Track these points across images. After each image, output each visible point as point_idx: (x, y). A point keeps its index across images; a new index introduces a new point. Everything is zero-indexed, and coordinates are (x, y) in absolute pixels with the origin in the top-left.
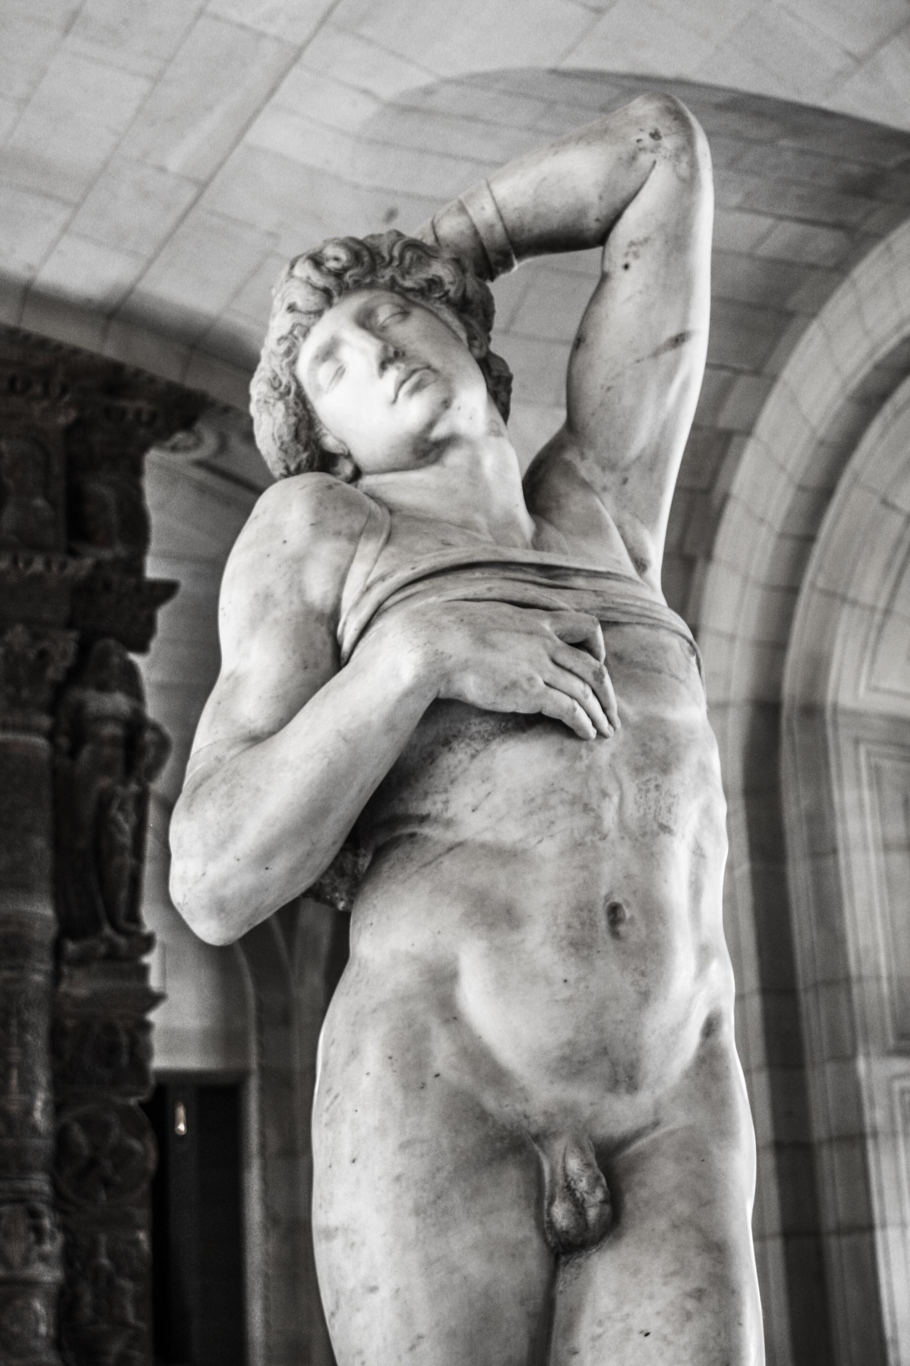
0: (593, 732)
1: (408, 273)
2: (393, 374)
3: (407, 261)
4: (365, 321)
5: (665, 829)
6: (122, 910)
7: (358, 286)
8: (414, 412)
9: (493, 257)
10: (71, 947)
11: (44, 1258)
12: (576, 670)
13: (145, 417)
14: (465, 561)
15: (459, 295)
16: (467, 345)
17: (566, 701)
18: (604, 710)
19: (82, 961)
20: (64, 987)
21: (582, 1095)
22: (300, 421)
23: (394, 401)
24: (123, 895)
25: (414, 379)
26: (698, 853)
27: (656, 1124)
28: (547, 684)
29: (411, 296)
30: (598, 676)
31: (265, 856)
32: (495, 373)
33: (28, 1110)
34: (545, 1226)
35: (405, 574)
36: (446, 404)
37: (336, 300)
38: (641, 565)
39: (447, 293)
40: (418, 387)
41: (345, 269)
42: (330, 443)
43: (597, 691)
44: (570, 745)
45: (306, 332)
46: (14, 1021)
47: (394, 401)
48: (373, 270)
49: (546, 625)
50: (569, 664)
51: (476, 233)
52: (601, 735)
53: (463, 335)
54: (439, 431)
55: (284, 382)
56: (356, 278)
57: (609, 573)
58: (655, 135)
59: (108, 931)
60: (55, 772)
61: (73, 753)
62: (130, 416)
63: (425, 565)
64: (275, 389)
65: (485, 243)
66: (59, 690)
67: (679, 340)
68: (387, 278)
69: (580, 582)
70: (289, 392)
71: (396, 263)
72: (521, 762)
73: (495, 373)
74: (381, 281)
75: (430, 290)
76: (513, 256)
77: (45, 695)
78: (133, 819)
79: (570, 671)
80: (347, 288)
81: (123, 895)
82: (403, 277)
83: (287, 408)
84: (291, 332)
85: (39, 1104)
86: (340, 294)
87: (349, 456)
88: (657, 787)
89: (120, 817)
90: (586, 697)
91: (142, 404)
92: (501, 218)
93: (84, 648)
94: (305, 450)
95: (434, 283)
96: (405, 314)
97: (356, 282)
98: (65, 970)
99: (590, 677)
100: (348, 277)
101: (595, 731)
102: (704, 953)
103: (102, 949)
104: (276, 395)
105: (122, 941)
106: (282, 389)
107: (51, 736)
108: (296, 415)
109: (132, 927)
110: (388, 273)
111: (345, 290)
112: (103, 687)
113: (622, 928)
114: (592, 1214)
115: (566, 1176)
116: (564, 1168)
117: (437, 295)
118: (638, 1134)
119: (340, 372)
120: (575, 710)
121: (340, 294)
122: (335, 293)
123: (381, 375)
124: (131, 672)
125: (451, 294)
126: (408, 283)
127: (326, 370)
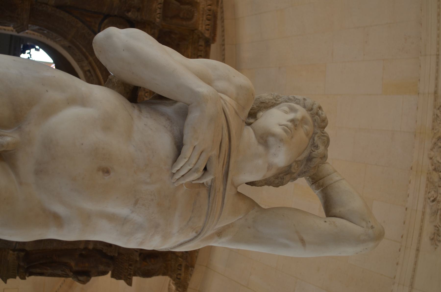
0: (174, 171)
1: (319, 139)
2: (289, 124)
3: (323, 138)
4: (303, 120)
5: (136, 203)
7: (314, 121)
8: (278, 130)
9: (321, 181)
10: (23, 254)
12: (199, 161)
13: (179, 277)
14: (232, 135)
15: (314, 156)
16: (297, 160)
17: (188, 155)
18: (183, 176)
20: (11, 252)
22: (267, 104)
23: (280, 125)
24: (38, 271)
25: (289, 130)
26: (124, 221)
27: (21, 183)
28: (195, 147)
29: (312, 140)
30: (197, 171)
31: (129, 49)
32: (285, 177)
36: (281, 140)
37: (309, 112)
38: (219, 234)
39: (314, 151)
40: (285, 131)
41: (319, 116)
42: (260, 114)
43: (190, 171)
44: (170, 161)
45: (297, 103)
47: (280, 125)
49: (215, 152)
50: (202, 158)
51: (329, 175)
53: (300, 158)
54: (271, 140)
55: (280, 100)
56: (317, 120)
57: (224, 204)
58: (372, 227)
62: (179, 272)
63: (231, 119)
64: (277, 97)
65: (325, 178)
67: (303, 242)
68: (317, 131)
69: (222, 189)
70: (276, 101)
71: (322, 134)
72: (164, 142)
73: (285, 177)
74: (316, 129)
75: (315, 146)
76: (322, 189)
79: (199, 159)
80: (313, 117)
81: (38, 271)
82: (318, 137)
83: (271, 99)
84: (297, 99)
86: (311, 114)
87: (256, 120)
88: (152, 200)
90: (189, 166)
91: (183, 275)
92: (335, 182)
93: (112, 258)
94: (257, 106)
95: (317, 147)
96: (307, 135)
97: (315, 120)
98: (16, 253)
99: (196, 167)
100: (317, 116)
101: (175, 172)
102: (87, 218)
104: (275, 97)
106: (277, 99)
108: (269, 102)
109: (28, 275)
110: (319, 131)
111: (312, 116)
113: (101, 173)
115: (4, 136)
116: (7, 136)
117: (313, 149)
118: (17, 174)
119: (286, 112)
120: (185, 158)
121: (311, 114)
122: (311, 112)
123: (288, 121)
125: (314, 153)
126: (316, 138)
127: (286, 108)
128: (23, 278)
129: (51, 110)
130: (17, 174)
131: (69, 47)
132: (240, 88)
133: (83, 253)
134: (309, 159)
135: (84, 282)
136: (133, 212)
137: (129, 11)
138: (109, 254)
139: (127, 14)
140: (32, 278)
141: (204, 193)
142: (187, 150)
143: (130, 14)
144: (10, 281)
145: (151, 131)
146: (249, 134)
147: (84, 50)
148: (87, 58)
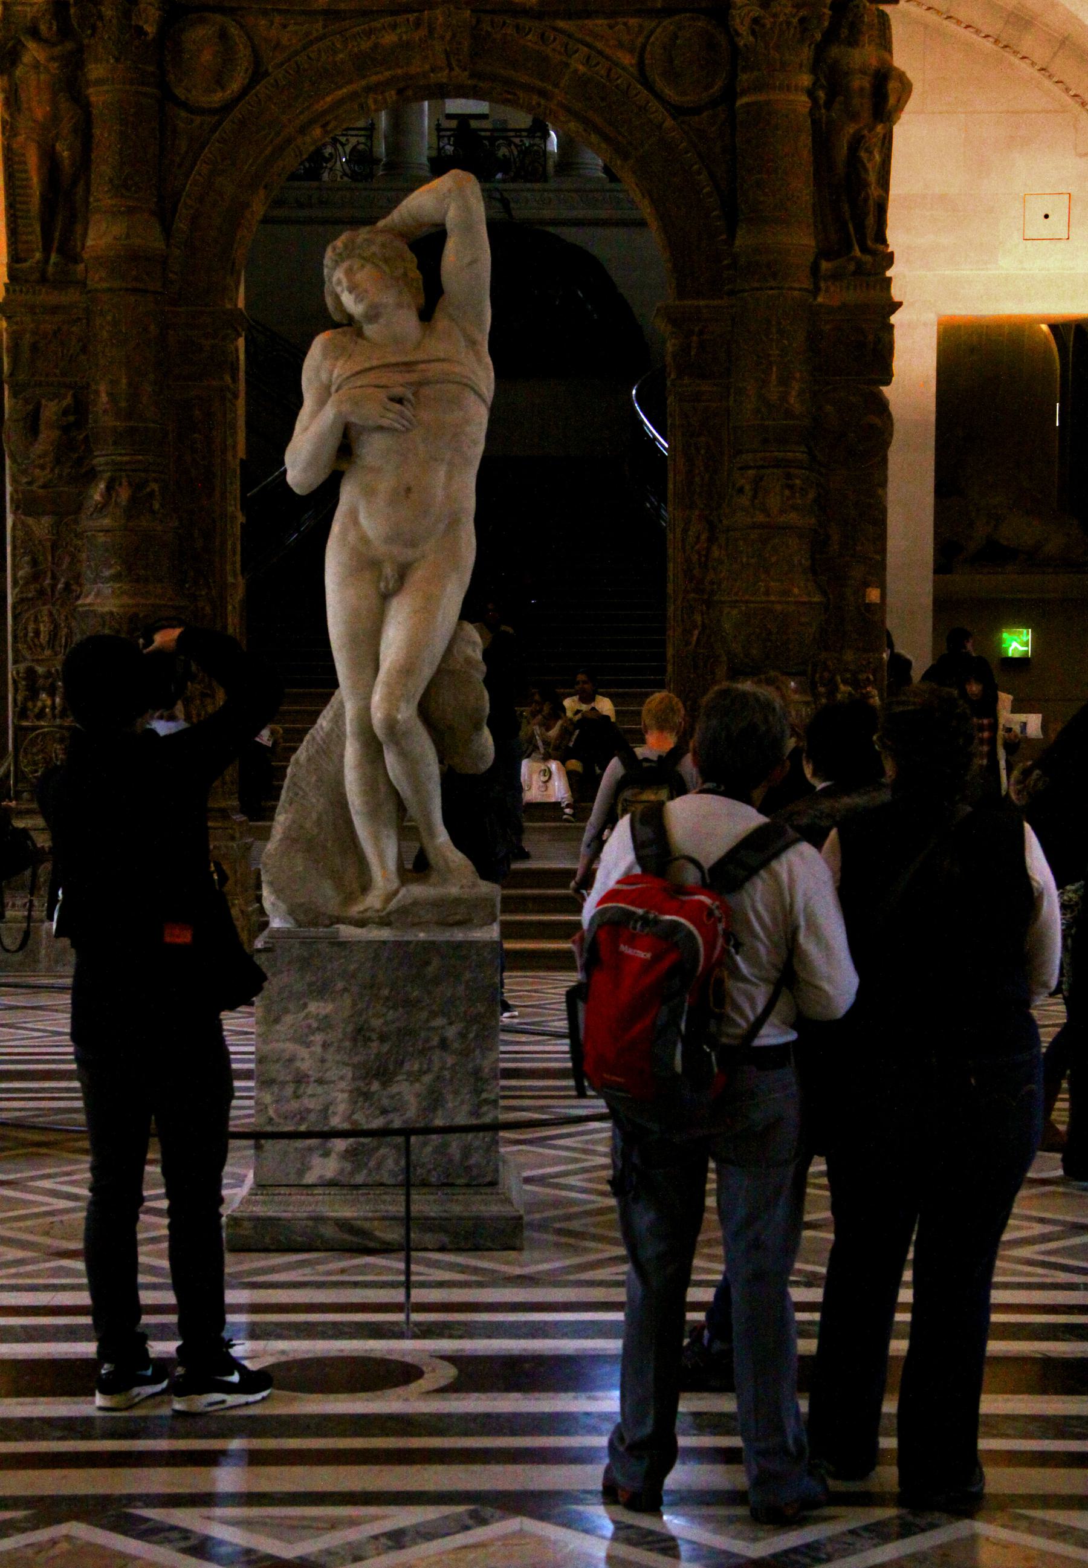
6: (870, 232)
7: (349, 257)
10: (825, 265)
11: (794, 508)
19: (836, 276)
21: (395, 550)
33: (784, 398)
34: (378, 588)
35: (348, 374)
38: (472, 343)
46: (774, 330)
48: (353, 249)
52: (408, 430)
59: (857, 252)
60: (814, 122)
61: (828, 105)
66: (820, 50)
77: (806, 53)
78: (877, 157)
81: (871, 220)
85: (794, 393)
89: (863, 154)
96: (363, 266)
98: (822, 285)
103: (852, 267)
105: (868, 258)
107: (811, 93)
110: (357, 252)
111: (343, 261)
112: (853, 41)
114: (391, 586)
118: (416, 560)
119: (342, 291)
124: (884, 22)
128: (889, 259)
129: (364, 539)
130: (416, 560)
131: (265, 187)
132: (325, 355)
133: (822, 102)
134: (386, 261)
135: (906, 88)
136: (442, 460)
137: (140, 31)
138: (826, 24)
139: (151, 36)
140: (891, 235)
141: (426, 391)
142: (385, 422)
143: (150, 29)
144: (896, 293)
145: (373, 450)
146: (369, 330)
147: (267, 152)
148: (289, 141)
